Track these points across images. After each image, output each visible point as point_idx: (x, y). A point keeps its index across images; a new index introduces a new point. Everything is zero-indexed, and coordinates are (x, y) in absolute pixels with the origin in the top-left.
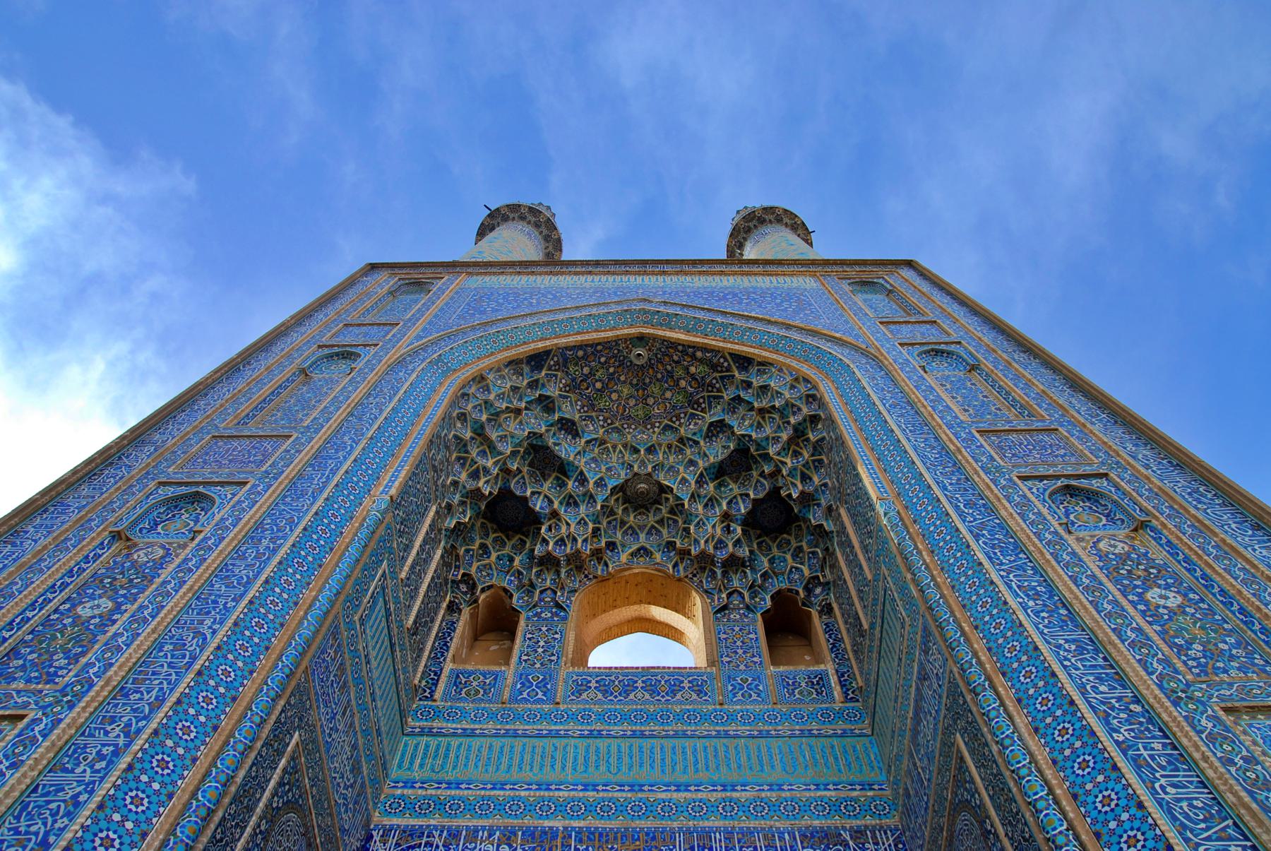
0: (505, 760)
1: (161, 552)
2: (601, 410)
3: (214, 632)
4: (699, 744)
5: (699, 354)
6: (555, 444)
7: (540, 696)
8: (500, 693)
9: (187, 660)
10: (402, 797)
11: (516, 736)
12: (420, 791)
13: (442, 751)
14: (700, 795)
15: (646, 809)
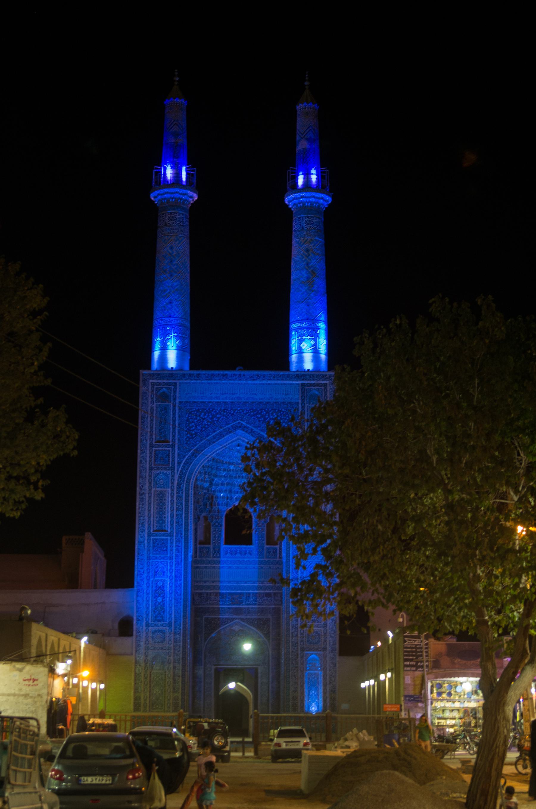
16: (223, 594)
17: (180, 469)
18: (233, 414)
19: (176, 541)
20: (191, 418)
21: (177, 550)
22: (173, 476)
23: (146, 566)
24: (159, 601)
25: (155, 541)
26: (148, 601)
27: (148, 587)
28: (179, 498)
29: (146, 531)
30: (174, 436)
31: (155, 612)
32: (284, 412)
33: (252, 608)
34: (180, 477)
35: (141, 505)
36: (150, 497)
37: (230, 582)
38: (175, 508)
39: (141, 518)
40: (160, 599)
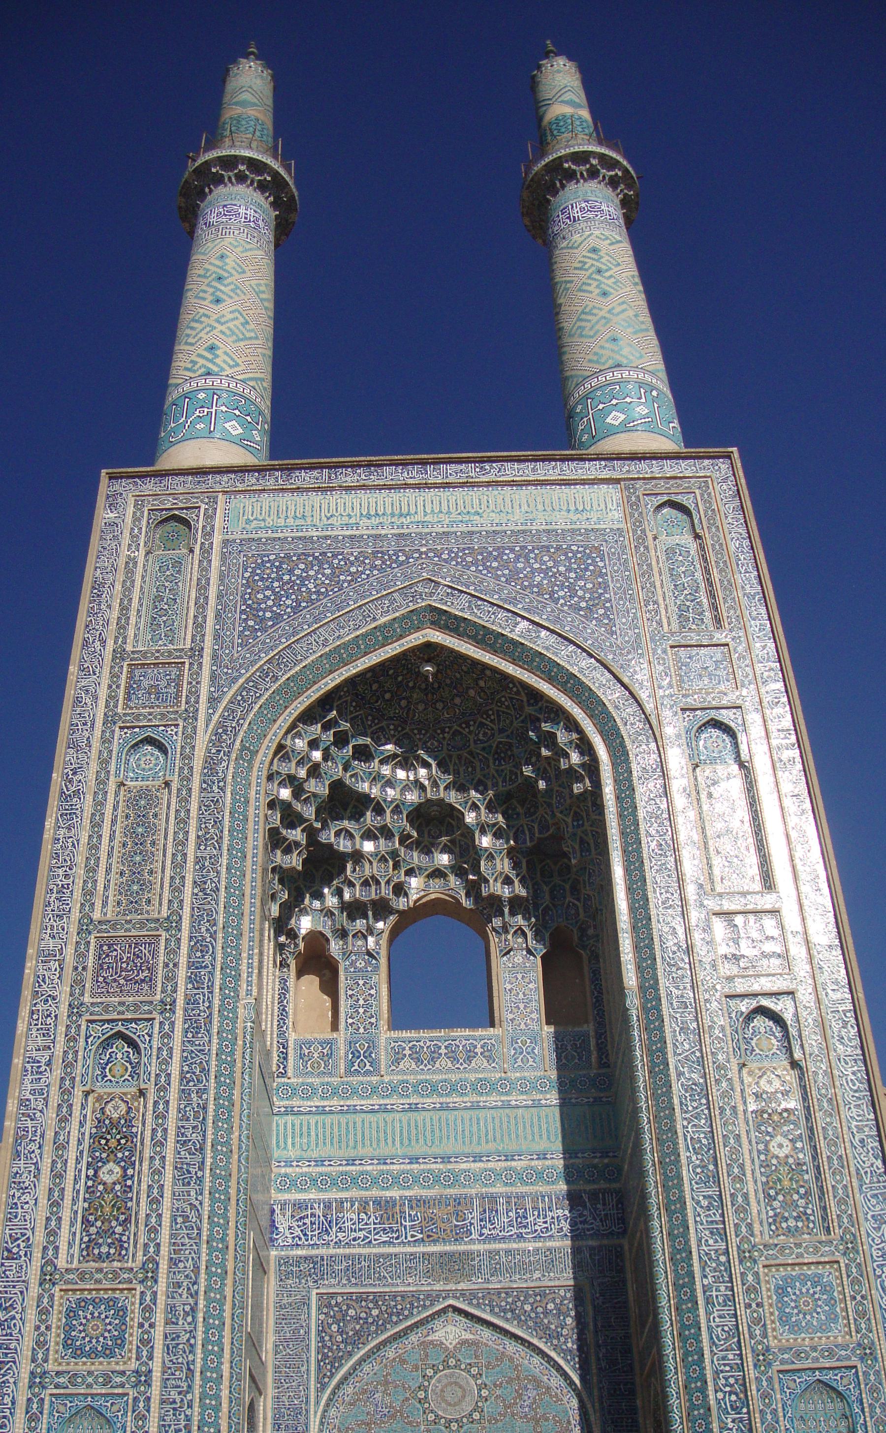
0: (351, 1136)
1: (123, 1107)
2: (391, 719)
3: (201, 1204)
4: (489, 1114)
5: (488, 673)
6: (351, 776)
7: (368, 1067)
8: (336, 1066)
9: (196, 1232)
10: (286, 1175)
11: (355, 1112)
12: (297, 1169)
13: (305, 1129)
14: (490, 1165)
15: (453, 1179)
16: (390, 1203)
17: (215, 718)
18: (402, 564)
19: (191, 949)
20: (262, 579)
21: (194, 980)
22: (190, 737)
23: (61, 1039)
24: (109, 1179)
25: (107, 945)
26: (58, 1176)
27: (63, 1120)
28: (211, 806)
29: (76, 915)
30: (199, 626)
31: (85, 1221)
32: (575, 553)
33: (508, 1252)
34: (217, 739)
35: (62, 832)
36: (99, 804)
37: (414, 1160)
38: (192, 837)
39: (61, 872)
40: (111, 1173)
